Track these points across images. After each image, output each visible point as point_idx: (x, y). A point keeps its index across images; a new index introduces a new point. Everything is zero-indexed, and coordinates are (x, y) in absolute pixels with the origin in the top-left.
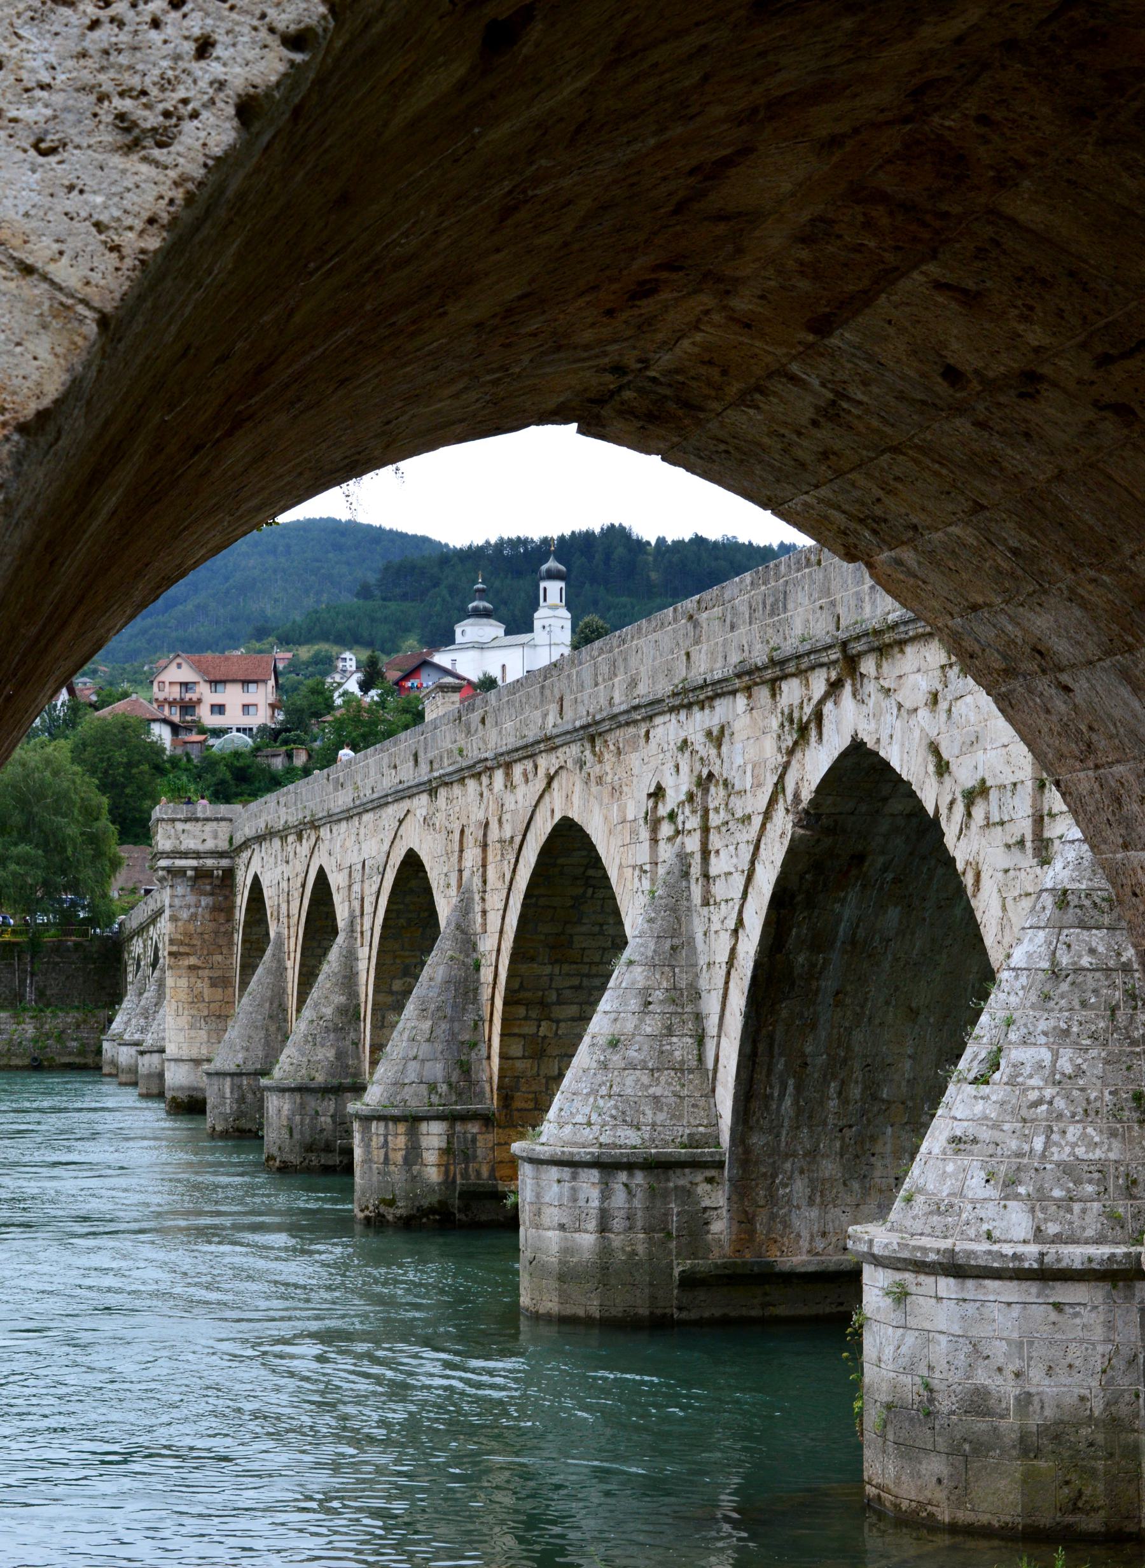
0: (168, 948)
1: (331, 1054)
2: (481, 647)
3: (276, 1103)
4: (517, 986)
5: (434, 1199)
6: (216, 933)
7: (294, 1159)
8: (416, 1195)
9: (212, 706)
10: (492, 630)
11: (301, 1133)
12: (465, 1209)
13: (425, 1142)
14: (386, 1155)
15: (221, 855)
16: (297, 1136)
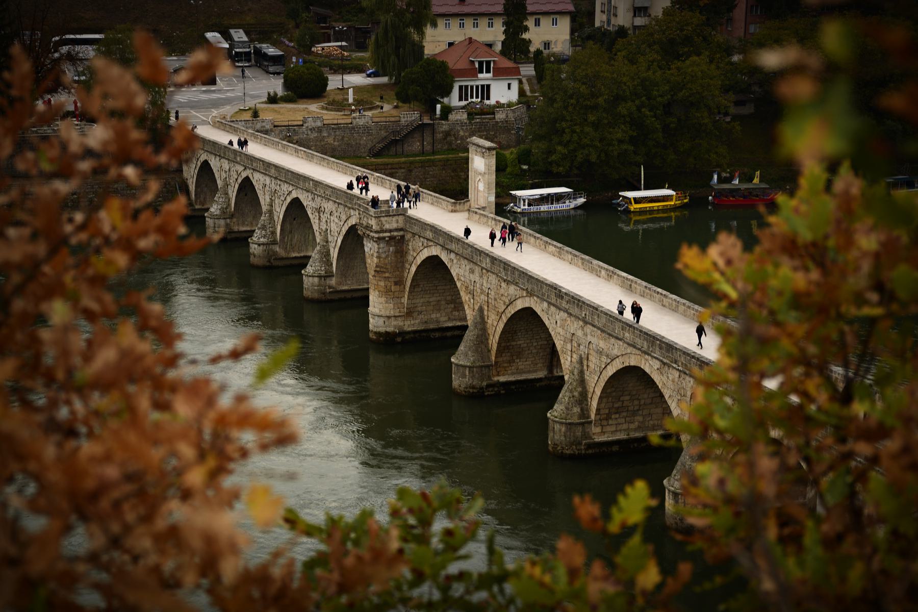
3: (558, 426)
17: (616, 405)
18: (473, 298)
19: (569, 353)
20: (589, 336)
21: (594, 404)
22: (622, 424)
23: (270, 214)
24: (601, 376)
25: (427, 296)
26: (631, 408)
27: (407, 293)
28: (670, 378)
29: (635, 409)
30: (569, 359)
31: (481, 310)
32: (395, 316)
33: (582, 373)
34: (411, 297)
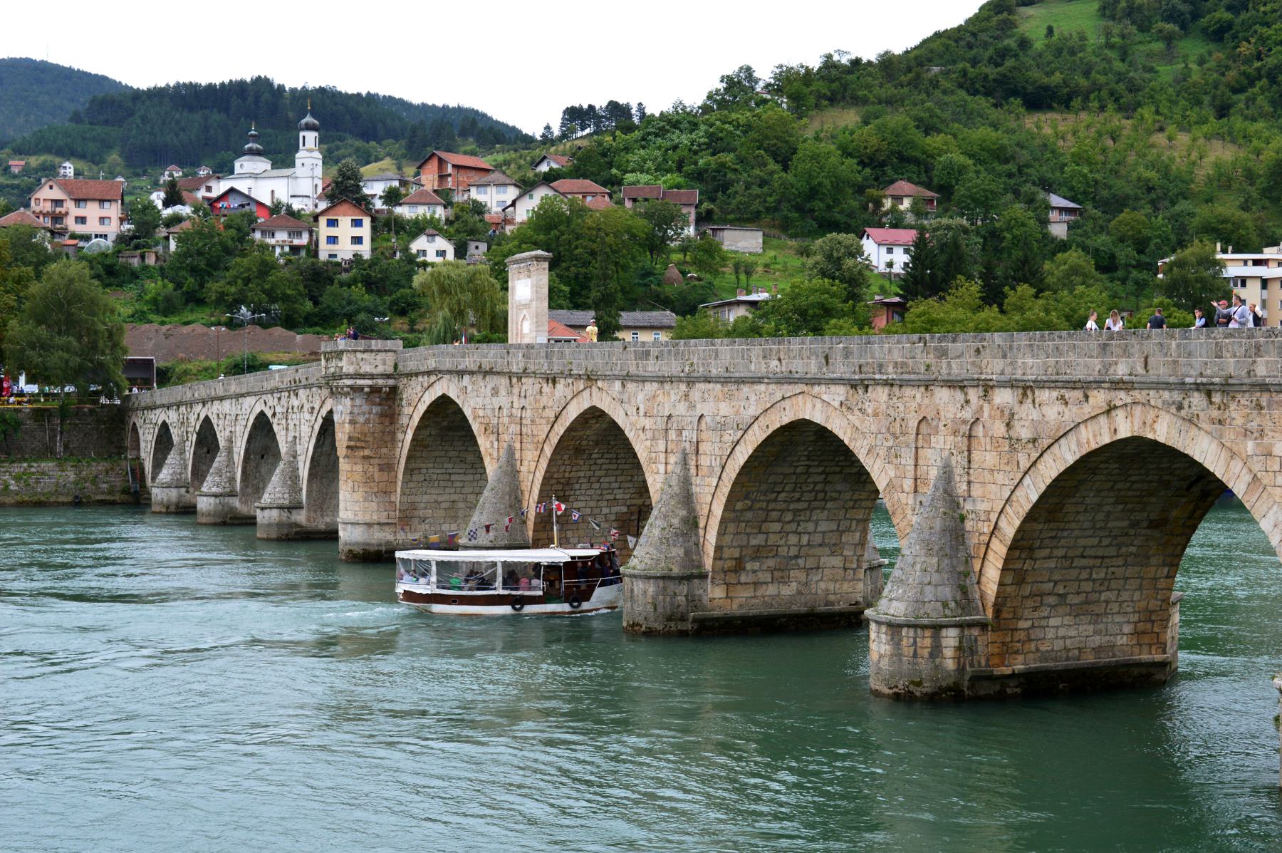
0: (345, 445)
1: (681, 552)
2: (255, 177)
4: (1019, 537)
5: (950, 681)
6: (383, 432)
7: (658, 626)
8: (938, 679)
9: (76, 218)
10: (262, 165)
11: (664, 607)
12: (971, 687)
13: (944, 642)
14: (915, 651)
15: (388, 376)
16: (660, 610)
17: (754, 542)
18: (498, 440)
19: (662, 456)
20: (698, 406)
21: (712, 538)
22: (766, 583)
23: (229, 452)
24: (724, 475)
25: (433, 491)
26: (783, 551)
27: (399, 484)
28: (870, 411)
29: (791, 554)
30: (662, 468)
31: (511, 452)
32: (379, 524)
33: (686, 483)
34: (407, 491)
